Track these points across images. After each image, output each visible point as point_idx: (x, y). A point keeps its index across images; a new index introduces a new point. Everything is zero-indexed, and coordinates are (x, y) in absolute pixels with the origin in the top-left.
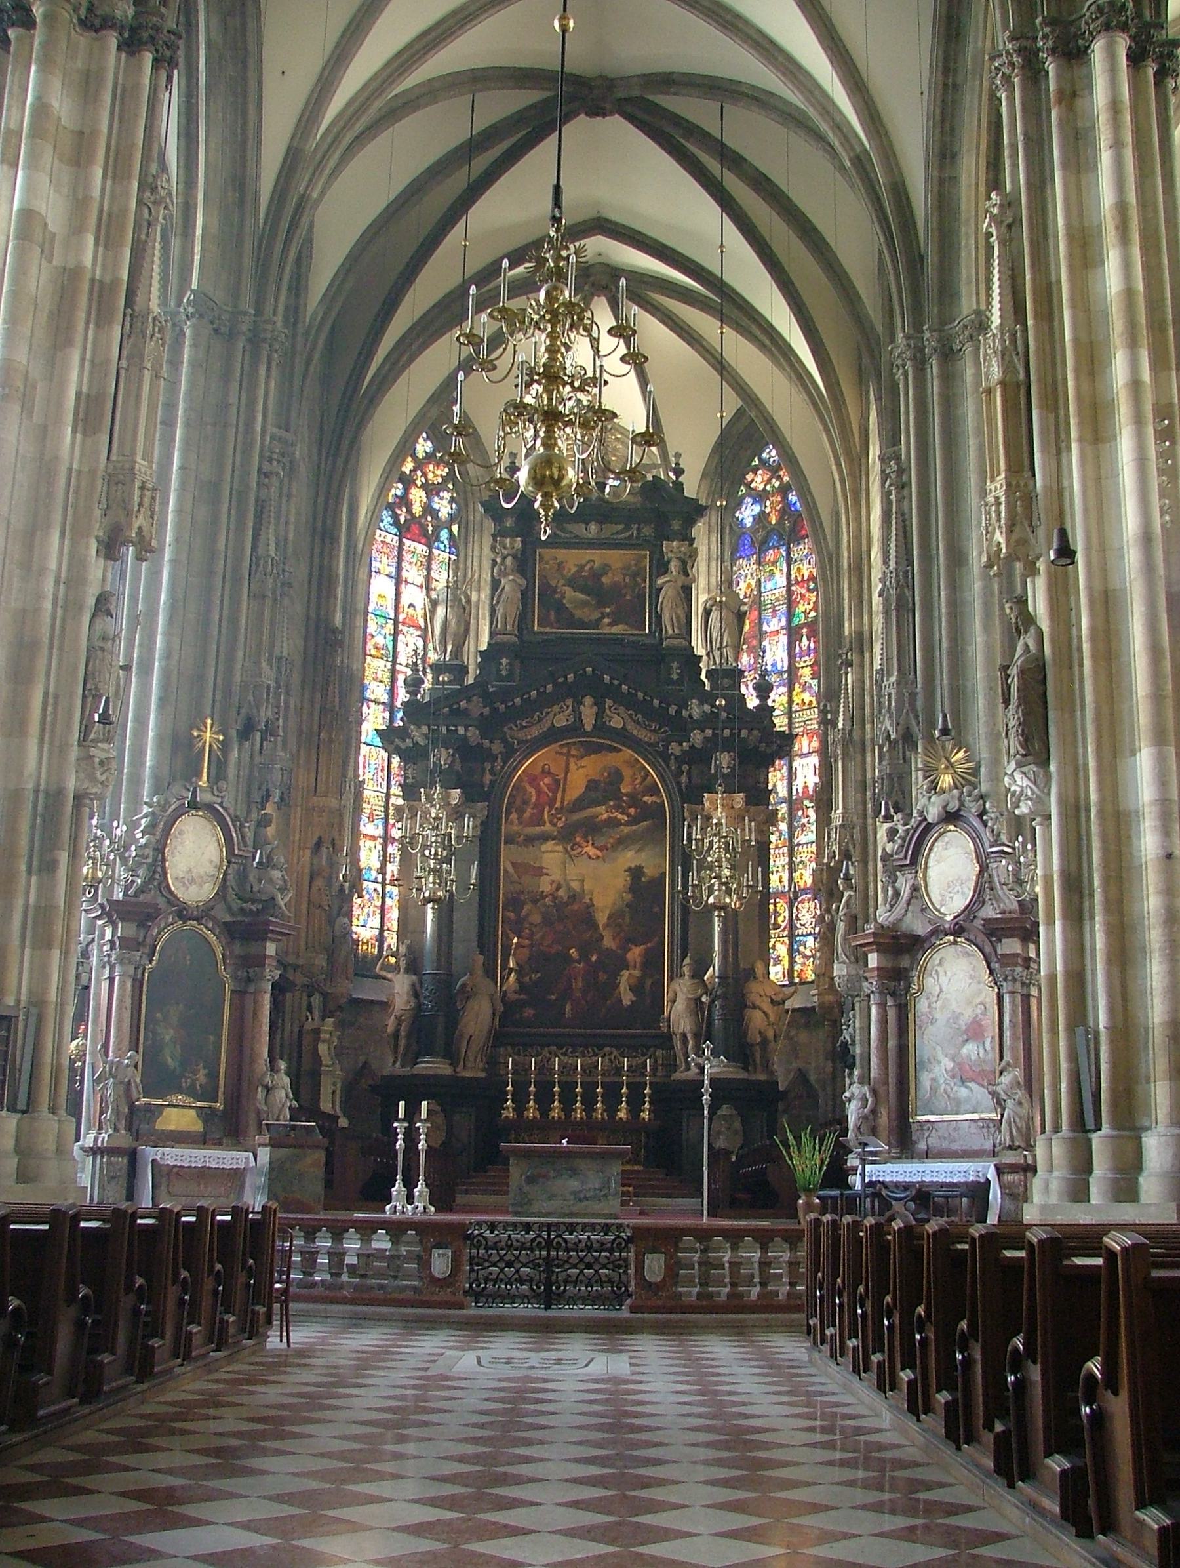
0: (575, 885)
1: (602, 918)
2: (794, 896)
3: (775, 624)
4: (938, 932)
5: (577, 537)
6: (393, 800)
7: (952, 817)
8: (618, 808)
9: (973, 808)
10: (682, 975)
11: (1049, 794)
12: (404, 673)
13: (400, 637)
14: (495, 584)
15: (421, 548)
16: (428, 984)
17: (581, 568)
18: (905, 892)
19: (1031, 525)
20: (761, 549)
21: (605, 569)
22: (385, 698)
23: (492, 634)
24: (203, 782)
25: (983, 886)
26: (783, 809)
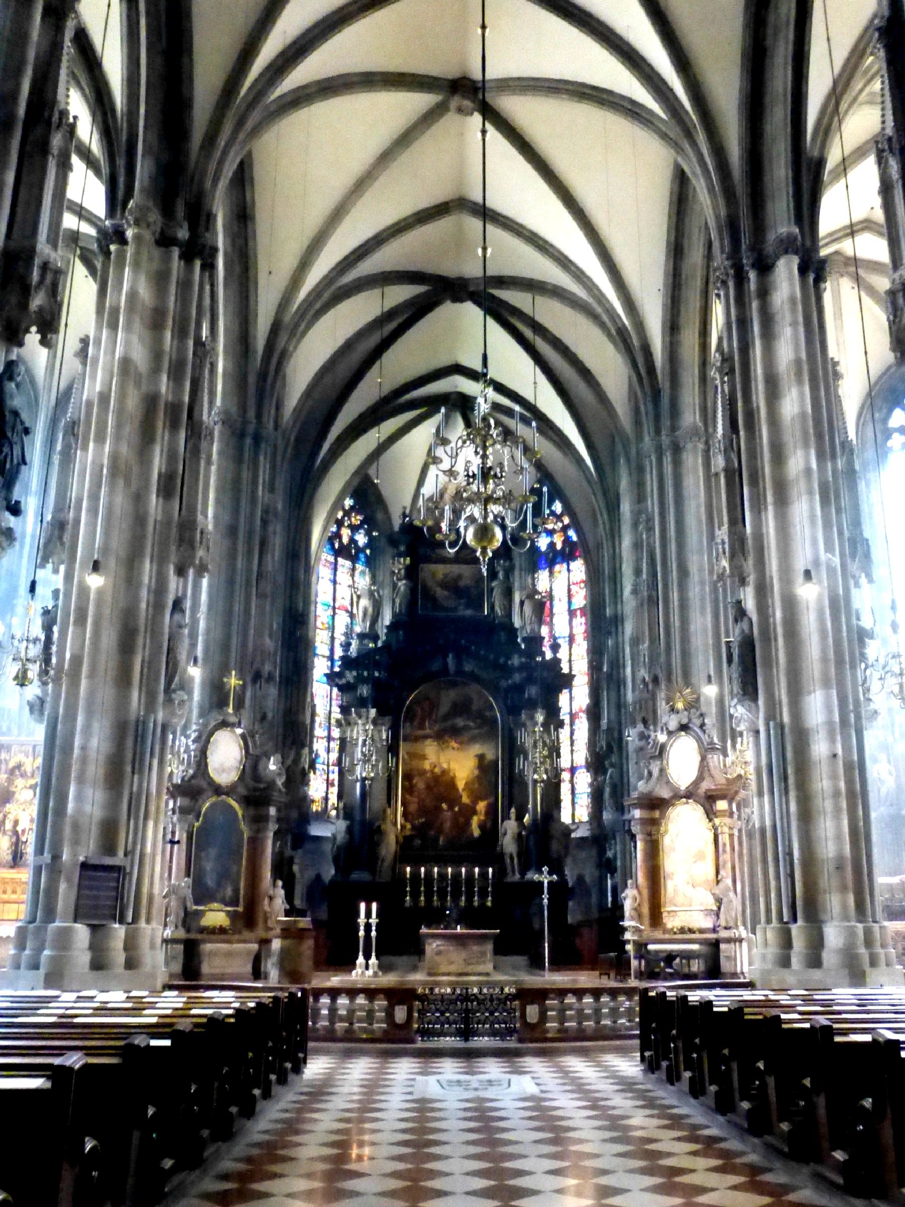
0: (445, 766)
1: (461, 785)
2: (573, 770)
3: (560, 608)
4: (679, 796)
5: (444, 557)
6: (333, 715)
7: (684, 728)
8: (468, 719)
9: (697, 722)
10: (509, 819)
11: (758, 718)
12: (340, 638)
13: (336, 617)
14: (395, 586)
15: (348, 564)
16: (357, 828)
17: (446, 575)
18: (656, 772)
19: (744, 555)
20: (551, 565)
21: (460, 577)
22: (328, 653)
23: (394, 615)
24: (230, 710)
25: (704, 769)
26: (567, 720)
